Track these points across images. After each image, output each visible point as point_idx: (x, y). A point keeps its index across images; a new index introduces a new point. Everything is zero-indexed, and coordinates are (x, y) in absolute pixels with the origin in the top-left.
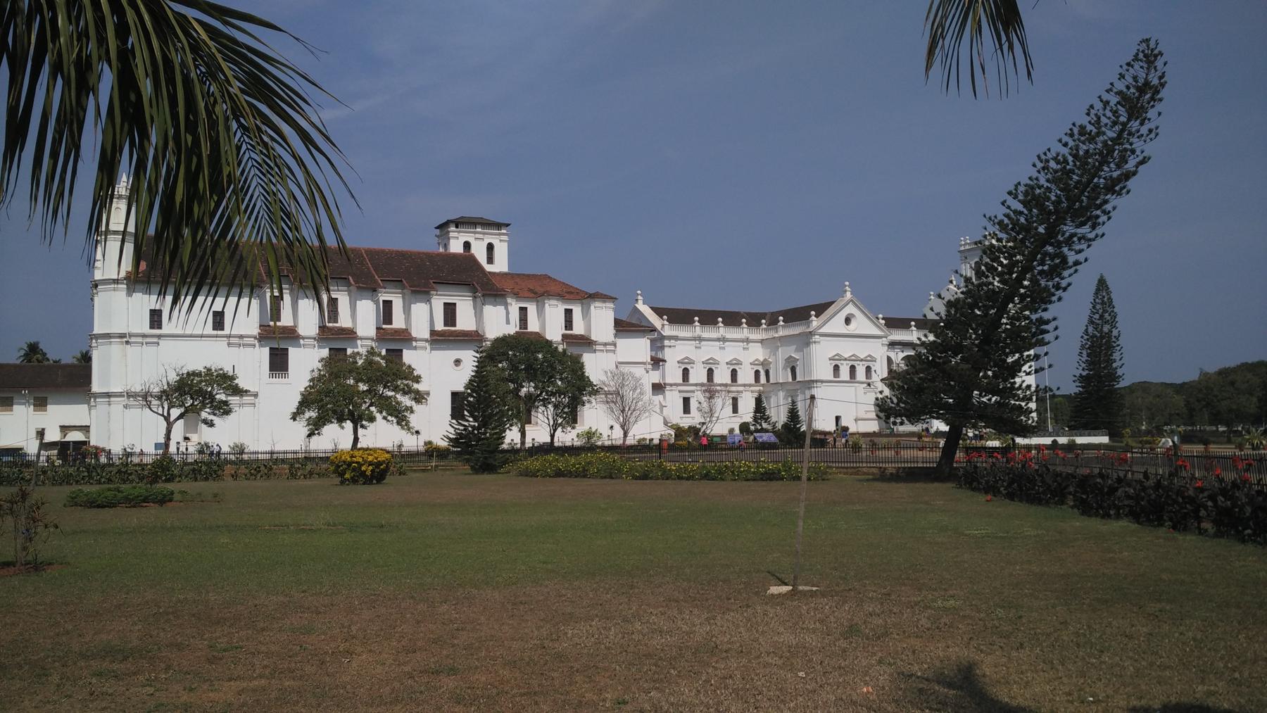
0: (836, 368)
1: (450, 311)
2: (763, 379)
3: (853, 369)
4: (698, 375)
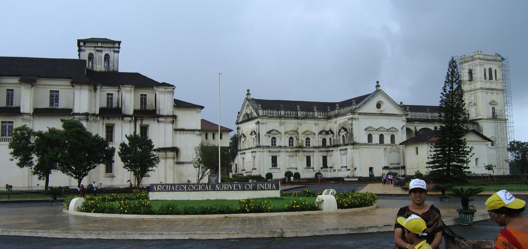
0: (370, 137)
1: (54, 97)
2: (328, 144)
3: (381, 137)
4: (283, 141)
